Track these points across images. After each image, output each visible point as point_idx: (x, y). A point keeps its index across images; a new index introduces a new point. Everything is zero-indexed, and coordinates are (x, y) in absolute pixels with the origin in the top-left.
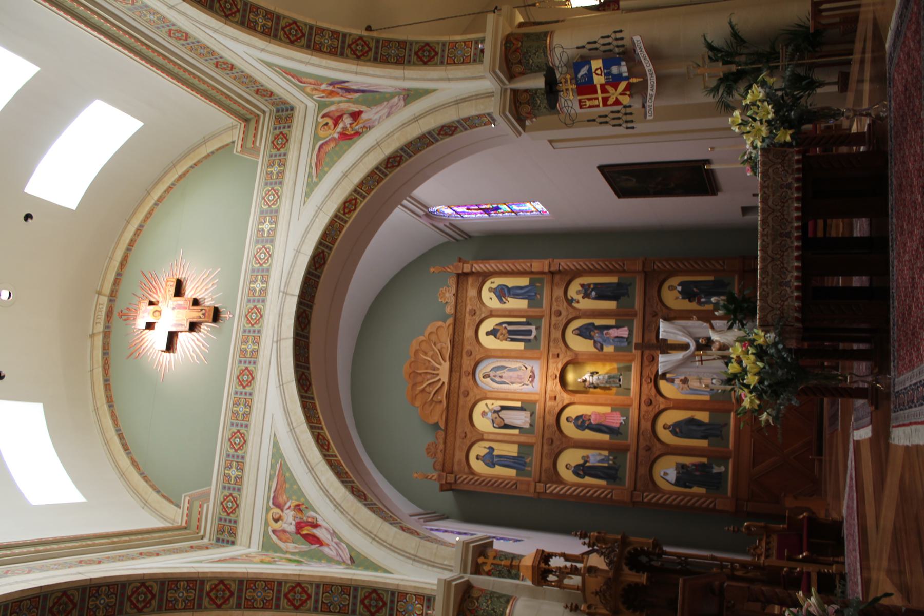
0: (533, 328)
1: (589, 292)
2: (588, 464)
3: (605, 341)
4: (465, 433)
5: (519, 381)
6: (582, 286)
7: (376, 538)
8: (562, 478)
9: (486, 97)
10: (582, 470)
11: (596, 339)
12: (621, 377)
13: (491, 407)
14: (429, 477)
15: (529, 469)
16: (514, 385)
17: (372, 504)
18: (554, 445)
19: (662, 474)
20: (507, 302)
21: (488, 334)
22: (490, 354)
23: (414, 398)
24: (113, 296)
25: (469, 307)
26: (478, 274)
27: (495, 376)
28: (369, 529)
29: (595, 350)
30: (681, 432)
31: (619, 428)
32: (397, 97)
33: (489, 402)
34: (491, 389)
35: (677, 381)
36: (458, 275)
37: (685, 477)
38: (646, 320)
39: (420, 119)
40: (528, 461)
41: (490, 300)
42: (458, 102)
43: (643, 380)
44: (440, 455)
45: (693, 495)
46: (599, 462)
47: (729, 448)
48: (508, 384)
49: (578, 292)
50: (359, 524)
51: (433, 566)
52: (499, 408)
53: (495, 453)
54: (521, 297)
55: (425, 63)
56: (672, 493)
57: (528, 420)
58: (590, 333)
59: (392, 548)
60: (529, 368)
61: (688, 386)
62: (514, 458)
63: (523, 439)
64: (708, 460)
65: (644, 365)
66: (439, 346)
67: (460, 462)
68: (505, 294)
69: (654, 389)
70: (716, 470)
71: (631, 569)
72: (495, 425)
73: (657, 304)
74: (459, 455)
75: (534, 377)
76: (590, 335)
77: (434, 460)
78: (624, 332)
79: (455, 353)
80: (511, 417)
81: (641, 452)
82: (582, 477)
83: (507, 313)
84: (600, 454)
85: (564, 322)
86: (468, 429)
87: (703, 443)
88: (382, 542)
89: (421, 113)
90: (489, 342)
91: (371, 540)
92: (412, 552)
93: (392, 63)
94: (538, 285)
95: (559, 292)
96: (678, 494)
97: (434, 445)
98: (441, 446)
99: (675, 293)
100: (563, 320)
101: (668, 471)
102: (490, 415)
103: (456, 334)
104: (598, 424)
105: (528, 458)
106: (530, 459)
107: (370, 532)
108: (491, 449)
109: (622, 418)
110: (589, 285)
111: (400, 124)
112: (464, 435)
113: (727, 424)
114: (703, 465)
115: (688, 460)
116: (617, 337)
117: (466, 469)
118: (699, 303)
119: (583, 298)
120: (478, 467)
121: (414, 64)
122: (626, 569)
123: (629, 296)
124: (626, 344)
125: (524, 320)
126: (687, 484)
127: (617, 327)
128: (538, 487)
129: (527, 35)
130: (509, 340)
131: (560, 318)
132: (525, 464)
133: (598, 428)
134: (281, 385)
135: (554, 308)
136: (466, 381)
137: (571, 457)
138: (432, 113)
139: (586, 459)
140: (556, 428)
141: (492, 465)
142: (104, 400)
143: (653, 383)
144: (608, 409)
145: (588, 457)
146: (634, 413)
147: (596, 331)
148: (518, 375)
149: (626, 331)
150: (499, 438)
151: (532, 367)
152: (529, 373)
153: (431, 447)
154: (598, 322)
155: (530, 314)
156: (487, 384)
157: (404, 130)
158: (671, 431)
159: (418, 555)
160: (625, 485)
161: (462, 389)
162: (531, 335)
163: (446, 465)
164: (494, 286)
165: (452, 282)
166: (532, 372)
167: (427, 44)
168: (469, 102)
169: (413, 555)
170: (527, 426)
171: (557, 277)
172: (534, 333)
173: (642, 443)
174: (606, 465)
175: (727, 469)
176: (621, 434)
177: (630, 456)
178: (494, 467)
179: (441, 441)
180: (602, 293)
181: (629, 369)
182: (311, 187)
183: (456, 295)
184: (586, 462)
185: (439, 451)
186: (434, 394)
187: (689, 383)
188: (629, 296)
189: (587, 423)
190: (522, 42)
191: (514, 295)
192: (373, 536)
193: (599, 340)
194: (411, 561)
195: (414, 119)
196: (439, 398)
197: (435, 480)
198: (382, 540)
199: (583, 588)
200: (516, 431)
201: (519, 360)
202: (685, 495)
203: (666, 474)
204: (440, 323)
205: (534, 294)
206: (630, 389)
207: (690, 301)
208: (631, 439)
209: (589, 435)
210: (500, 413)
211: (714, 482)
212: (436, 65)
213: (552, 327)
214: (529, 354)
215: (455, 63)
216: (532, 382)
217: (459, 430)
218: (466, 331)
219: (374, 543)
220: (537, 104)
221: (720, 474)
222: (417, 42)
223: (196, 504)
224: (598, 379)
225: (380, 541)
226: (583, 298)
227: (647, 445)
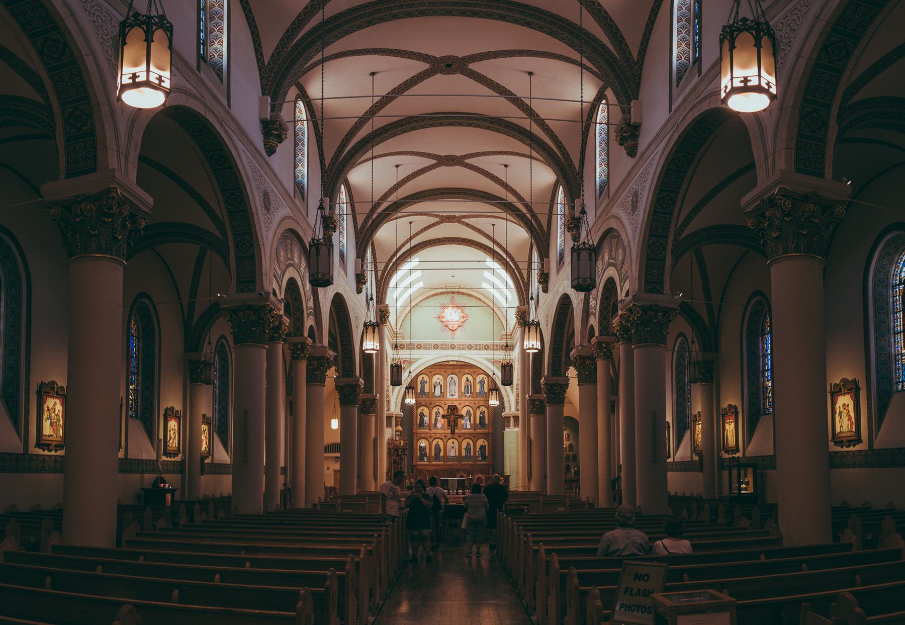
0: (469, 394)
6: (484, 411)
10: (422, 415)
21: (467, 378)
24: (459, 293)
33: (443, 380)
37: (422, 449)
41: (480, 377)
42: (509, 401)
45: (417, 452)
56: (417, 445)
57: (437, 395)
62: (424, 391)
63: (431, 394)
70: (425, 458)
78: (469, 426)
81: (429, 434)
86: (433, 373)
87: (433, 454)
90: (464, 379)
95: (482, 403)
96: (417, 448)
113: (440, 461)
114: (427, 454)
118: (479, 451)
127: (470, 424)
134: (434, 359)
136: (449, 371)
137: (426, 411)
142: (427, 296)
146: (442, 431)
154: (472, 418)
155: (474, 393)
156: (449, 379)
161: (447, 370)
172: (468, 395)
175: (425, 462)
180: (482, 419)
182: (488, 360)
200: (433, 391)
202: (416, 450)
208: (433, 431)
211: (421, 459)
221: (424, 460)
223: (401, 336)
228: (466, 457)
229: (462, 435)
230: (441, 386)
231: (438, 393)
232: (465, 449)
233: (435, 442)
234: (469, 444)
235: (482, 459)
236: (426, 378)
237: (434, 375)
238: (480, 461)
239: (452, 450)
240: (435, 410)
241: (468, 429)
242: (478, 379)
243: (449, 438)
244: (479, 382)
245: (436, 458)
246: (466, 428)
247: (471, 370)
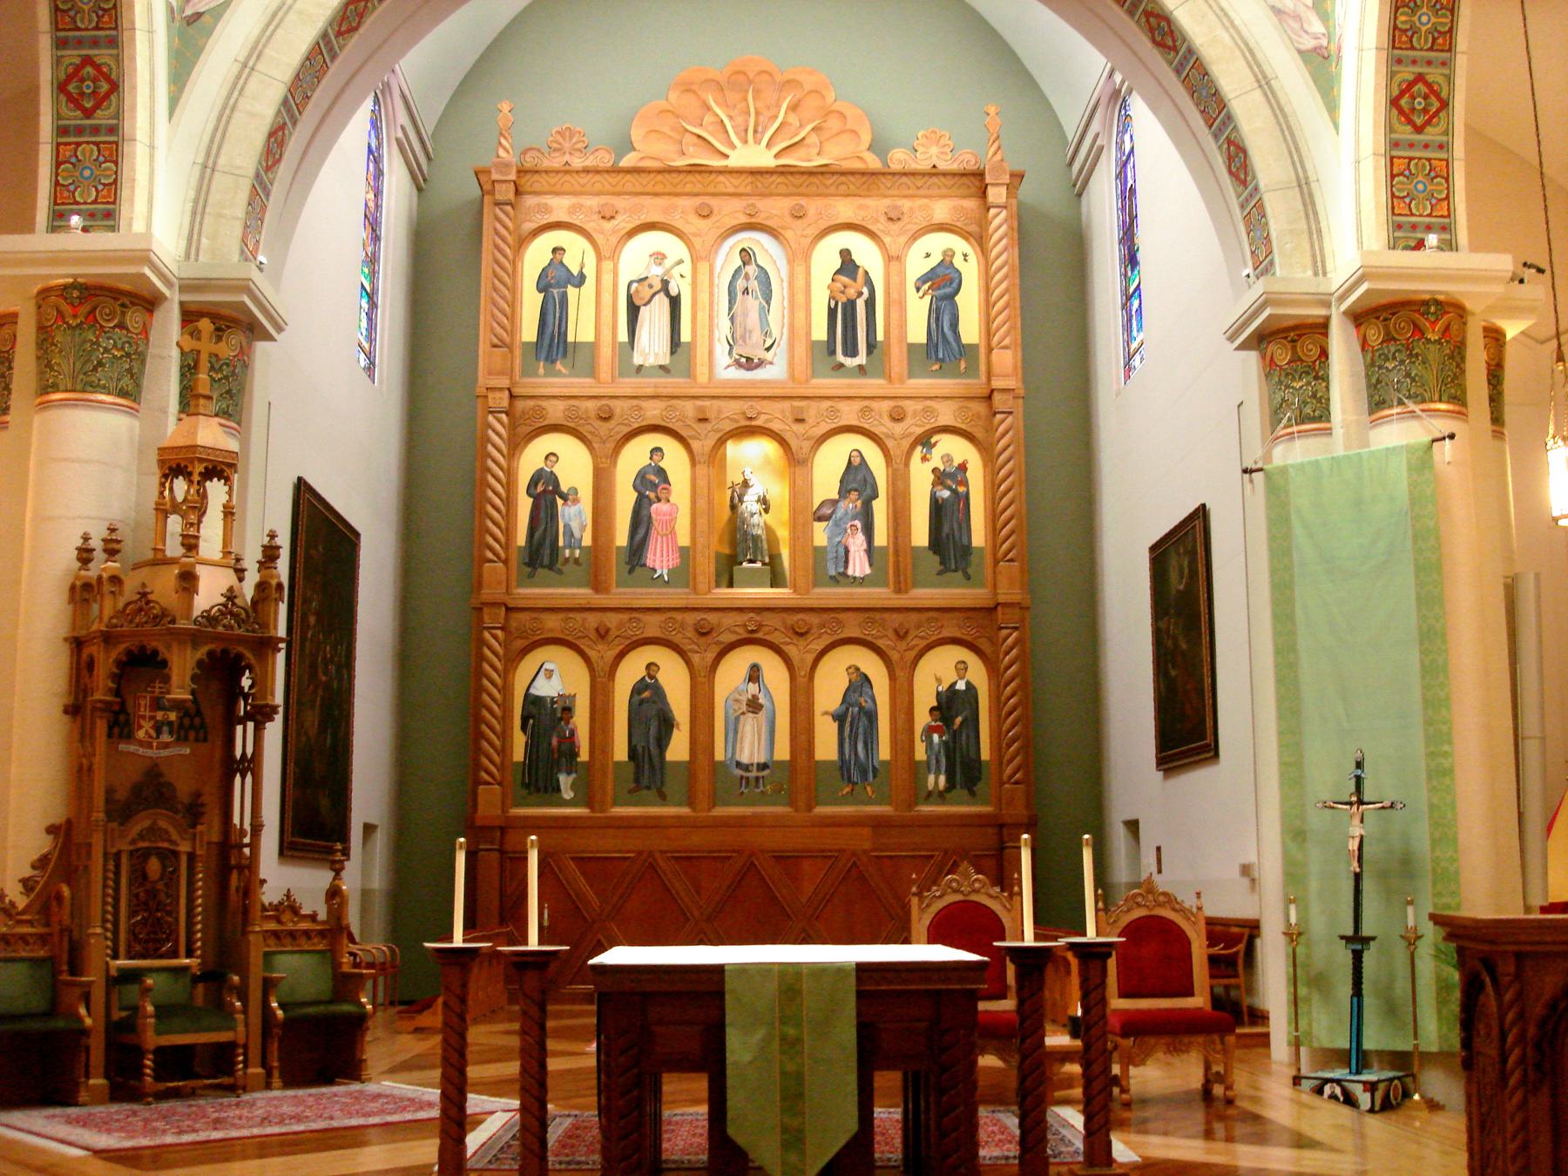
1: (949, 482)
2: (560, 502)
3: (837, 525)
4: (612, 217)
5: (738, 336)
6: (963, 467)
7: (247, 70)
8: (522, 452)
9: (1314, 256)
10: (547, 491)
11: (841, 504)
12: (759, 565)
13: (676, 272)
14: (503, 141)
15: (541, 371)
16: (729, 323)
17: (331, 50)
18: (598, 424)
19: (547, 666)
20: (921, 293)
21: (845, 254)
22: (800, 257)
23: (688, 88)
25: (906, 204)
26: (983, 223)
27: (747, 277)
28: (267, 51)
29: (816, 506)
30: (642, 702)
31: (645, 565)
32: (1323, 30)
33: (686, 268)
34: (717, 269)
35: (753, 688)
36: (979, 175)
38: (887, 616)
39: (1265, 95)
40: (559, 366)
43: (751, 615)
44: (556, 162)
45: (505, 736)
46: (567, 526)
47: (615, 804)
48: (730, 309)
49: (947, 458)
50: (277, 27)
51: (194, 213)
52: (673, 292)
53: (572, 291)
54: (934, 326)
55: (1394, 102)
56: (506, 689)
57: (651, 361)
58: (856, 490)
59: (228, 111)
60: (769, 356)
61: (743, 713)
62: (563, 334)
63: (606, 352)
64: (583, 763)
65: (784, 615)
66: (814, 139)
67: (547, 209)
68: (939, 288)
69: (733, 638)
70: (565, 780)
71: (200, 663)
72: (635, 285)
73: (922, 638)
74: (560, 207)
75: (749, 369)
76: (849, 492)
77: (546, 150)
78: (859, 566)
79: (798, 180)
80: (655, 317)
81: (592, 620)
82: (529, 491)
83: (895, 296)
84: (583, 528)
85: (877, 430)
87: (621, 752)
88: (239, 86)
89: (1280, 95)
91: (241, 59)
92: (222, 161)
93: (1395, 18)
94: (963, 365)
95: (947, 414)
96: (506, 706)
97: (580, 146)
98: (577, 162)
99: (949, 677)
100: (884, 427)
101: (555, 678)
102: (656, 271)
103: (843, 179)
104: (650, 516)
105: (564, 367)
106: (564, 371)
107: (258, 57)
108: (580, 280)
109: (665, 572)
110: (965, 483)
111: (1252, 44)
112: (608, 215)
113: (663, 798)
114: (574, 754)
115: (581, 721)
116: (847, 551)
117: (529, 226)
118: (929, 730)
119: (935, 470)
120: (536, 256)
121: (1391, 75)
122: (202, 652)
123: (940, 573)
124: (833, 573)
125: (880, 336)
126: (531, 721)
127: (870, 550)
128: (498, 395)
129: (1458, 352)
130: (833, 306)
131: (886, 420)
132: (550, 359)
133: (640, 520)
135: (910, 406)
136: (731, 211)
138: (1278, 123)
139: (569, 497)
140: (636, 425)
141: (543, 285)
143: (745, 635)
144: (684, 540)
145: (576, 501)
146: (676, 596)
147: (859, 503)
148: (750, 332)
149: (862, 569)
150: (607, 298)
151: (771, 363)
152: (758, 354)
153: (574, 140)
154: (880, 508)
157: (1238, 53)
158: (643, 678)
159: (217, 176)
160: (519, 586)
161: (714, 202)
162: (846, 354)
163: (536, 177)
164: (958, 262)
165: (965, 160)
166: (761, 363)
167: (1445, 104)
168: (1302, 213)
169: (215, 163)
170: (637, 359)
171: (980, 408)
172: (850, 362)
173: (612, 620)
174: (561, 543)
175: (566, 804)
176: (630, 572)
177: (582, 594)
178: (540, 291)
179: (590, 162)
181: (776, 580)
183: (934, 172)
184: (565, 498)
185: (567, 158)
186: (699, 136)
187: (751, 715)
188: (940, 573)
189: (652, 495)
190: (1439, 342)
191: (938, 309)
192: (251, 64)
193: (840, 513)
194: (200, 160)
195: (1265, 77)
196: (691, 149)
197: (498, 156)
198: (242, 89)
199: (160, 561)
200: (623, 336)
201: (785, 330)
202: (506, 718)
203: (550, 674)
204: (866, 138)
205: (941, 356)
206: (731, 585)
207: (932, 710)
209: (625, 500)
210: (662, 294)
212: (1390, 129)
213: (866, 403)
214: (801, 351)
215: (1393, 176)
216: (738, 364)
217: (621, 203)
218: (849, 200)
219: (236, 68)
220: (1293, 379)
222: (1449, 79)
224: (752, 515)
225: (242, 81)
226: (935, 470)
227: (608, 631)
228: (843, 765)
229: (814, 619)
230: (675, 303)
231: (652, 345)
232: (840, 718)
233: (631, 671)
234: (860, 683)
235: (951, 784)
236: (577, 253)
237: (632, 233)
238: (941, 796)
239: (751, 727)
240: (635, 456)
241: (855, 581)
242: (919, 261)
243: (728, 638)
244: (924, 279)
245: (637, 780)
246: (842, 578)
247: (870, 202)
